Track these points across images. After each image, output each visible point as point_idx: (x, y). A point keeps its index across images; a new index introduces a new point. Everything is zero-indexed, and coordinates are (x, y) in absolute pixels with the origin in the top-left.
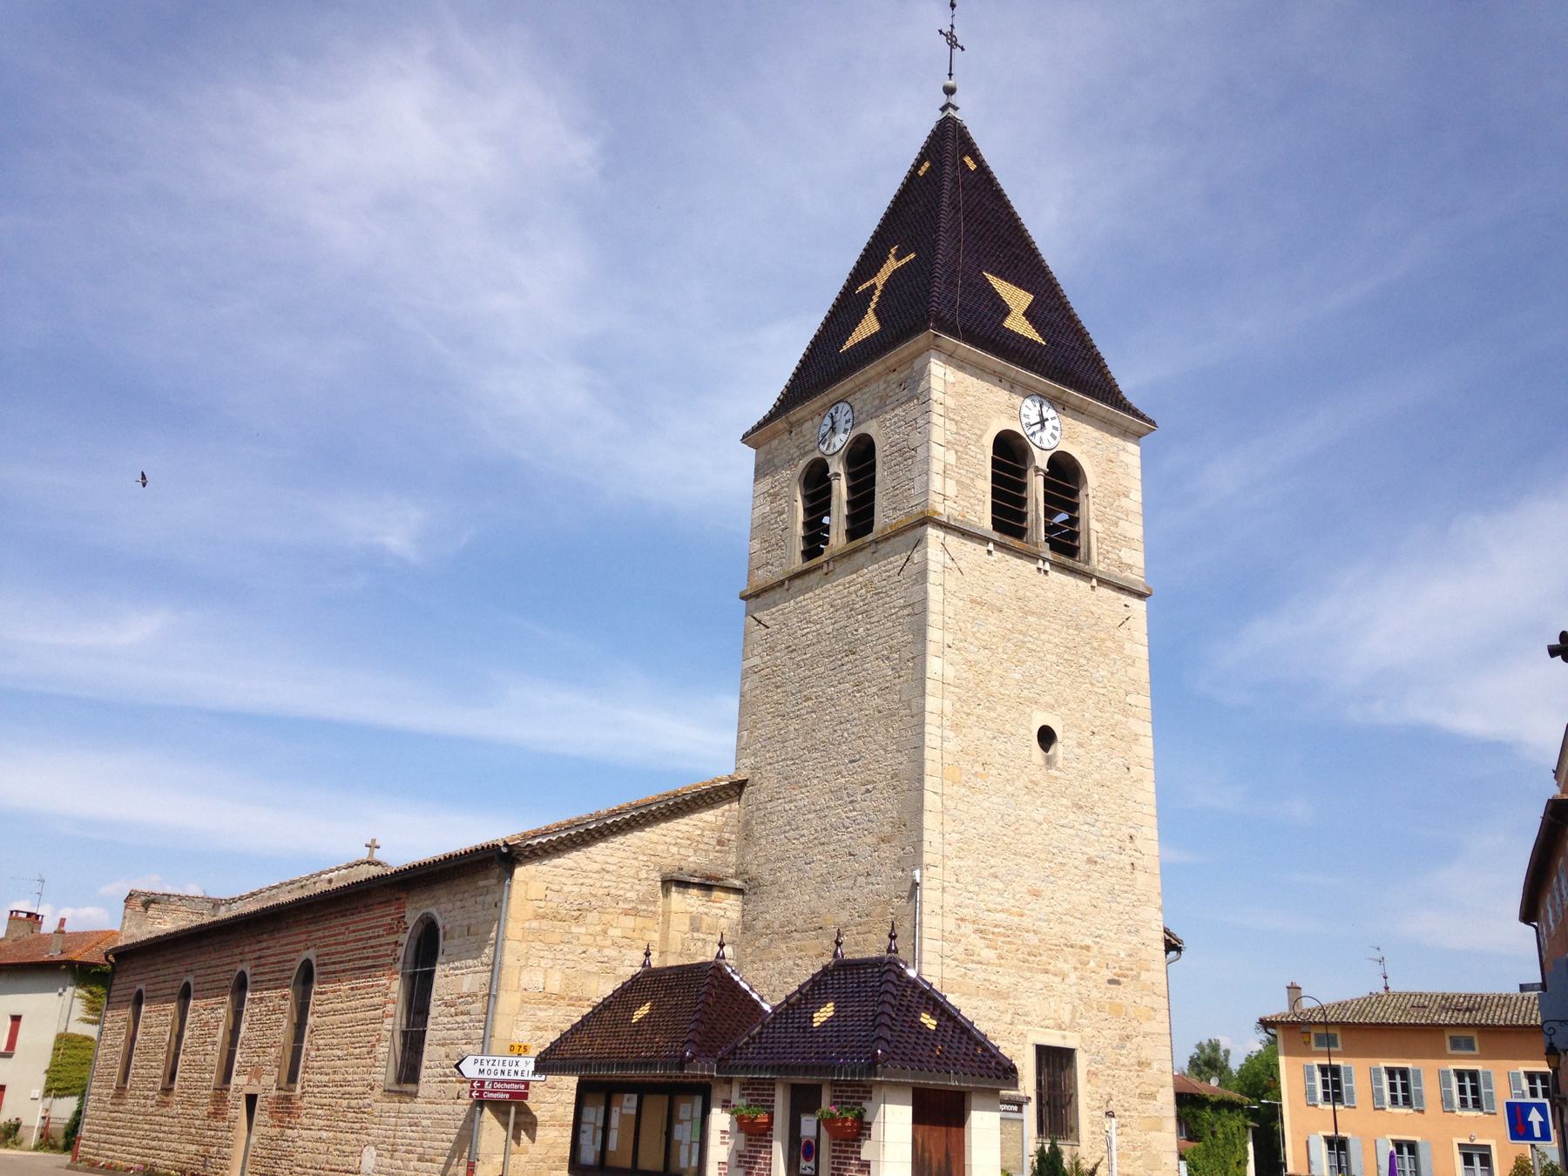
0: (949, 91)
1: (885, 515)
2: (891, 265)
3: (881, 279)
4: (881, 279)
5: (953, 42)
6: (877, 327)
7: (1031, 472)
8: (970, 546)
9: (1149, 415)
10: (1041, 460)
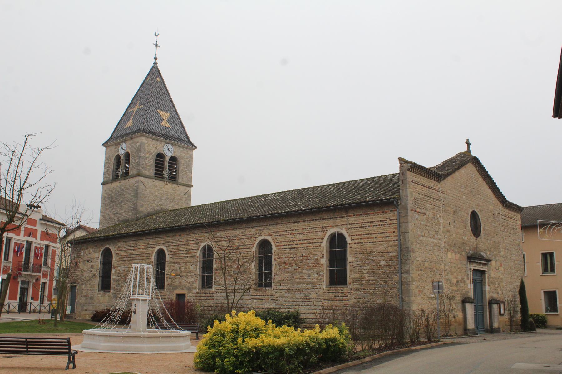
0: (156, 59)
1: (131, 172)
3: (135, 109)
4: (135, 109)
5: (156, 45)
6: (132, 124)
8: (150, 180)
10: (168, 159)
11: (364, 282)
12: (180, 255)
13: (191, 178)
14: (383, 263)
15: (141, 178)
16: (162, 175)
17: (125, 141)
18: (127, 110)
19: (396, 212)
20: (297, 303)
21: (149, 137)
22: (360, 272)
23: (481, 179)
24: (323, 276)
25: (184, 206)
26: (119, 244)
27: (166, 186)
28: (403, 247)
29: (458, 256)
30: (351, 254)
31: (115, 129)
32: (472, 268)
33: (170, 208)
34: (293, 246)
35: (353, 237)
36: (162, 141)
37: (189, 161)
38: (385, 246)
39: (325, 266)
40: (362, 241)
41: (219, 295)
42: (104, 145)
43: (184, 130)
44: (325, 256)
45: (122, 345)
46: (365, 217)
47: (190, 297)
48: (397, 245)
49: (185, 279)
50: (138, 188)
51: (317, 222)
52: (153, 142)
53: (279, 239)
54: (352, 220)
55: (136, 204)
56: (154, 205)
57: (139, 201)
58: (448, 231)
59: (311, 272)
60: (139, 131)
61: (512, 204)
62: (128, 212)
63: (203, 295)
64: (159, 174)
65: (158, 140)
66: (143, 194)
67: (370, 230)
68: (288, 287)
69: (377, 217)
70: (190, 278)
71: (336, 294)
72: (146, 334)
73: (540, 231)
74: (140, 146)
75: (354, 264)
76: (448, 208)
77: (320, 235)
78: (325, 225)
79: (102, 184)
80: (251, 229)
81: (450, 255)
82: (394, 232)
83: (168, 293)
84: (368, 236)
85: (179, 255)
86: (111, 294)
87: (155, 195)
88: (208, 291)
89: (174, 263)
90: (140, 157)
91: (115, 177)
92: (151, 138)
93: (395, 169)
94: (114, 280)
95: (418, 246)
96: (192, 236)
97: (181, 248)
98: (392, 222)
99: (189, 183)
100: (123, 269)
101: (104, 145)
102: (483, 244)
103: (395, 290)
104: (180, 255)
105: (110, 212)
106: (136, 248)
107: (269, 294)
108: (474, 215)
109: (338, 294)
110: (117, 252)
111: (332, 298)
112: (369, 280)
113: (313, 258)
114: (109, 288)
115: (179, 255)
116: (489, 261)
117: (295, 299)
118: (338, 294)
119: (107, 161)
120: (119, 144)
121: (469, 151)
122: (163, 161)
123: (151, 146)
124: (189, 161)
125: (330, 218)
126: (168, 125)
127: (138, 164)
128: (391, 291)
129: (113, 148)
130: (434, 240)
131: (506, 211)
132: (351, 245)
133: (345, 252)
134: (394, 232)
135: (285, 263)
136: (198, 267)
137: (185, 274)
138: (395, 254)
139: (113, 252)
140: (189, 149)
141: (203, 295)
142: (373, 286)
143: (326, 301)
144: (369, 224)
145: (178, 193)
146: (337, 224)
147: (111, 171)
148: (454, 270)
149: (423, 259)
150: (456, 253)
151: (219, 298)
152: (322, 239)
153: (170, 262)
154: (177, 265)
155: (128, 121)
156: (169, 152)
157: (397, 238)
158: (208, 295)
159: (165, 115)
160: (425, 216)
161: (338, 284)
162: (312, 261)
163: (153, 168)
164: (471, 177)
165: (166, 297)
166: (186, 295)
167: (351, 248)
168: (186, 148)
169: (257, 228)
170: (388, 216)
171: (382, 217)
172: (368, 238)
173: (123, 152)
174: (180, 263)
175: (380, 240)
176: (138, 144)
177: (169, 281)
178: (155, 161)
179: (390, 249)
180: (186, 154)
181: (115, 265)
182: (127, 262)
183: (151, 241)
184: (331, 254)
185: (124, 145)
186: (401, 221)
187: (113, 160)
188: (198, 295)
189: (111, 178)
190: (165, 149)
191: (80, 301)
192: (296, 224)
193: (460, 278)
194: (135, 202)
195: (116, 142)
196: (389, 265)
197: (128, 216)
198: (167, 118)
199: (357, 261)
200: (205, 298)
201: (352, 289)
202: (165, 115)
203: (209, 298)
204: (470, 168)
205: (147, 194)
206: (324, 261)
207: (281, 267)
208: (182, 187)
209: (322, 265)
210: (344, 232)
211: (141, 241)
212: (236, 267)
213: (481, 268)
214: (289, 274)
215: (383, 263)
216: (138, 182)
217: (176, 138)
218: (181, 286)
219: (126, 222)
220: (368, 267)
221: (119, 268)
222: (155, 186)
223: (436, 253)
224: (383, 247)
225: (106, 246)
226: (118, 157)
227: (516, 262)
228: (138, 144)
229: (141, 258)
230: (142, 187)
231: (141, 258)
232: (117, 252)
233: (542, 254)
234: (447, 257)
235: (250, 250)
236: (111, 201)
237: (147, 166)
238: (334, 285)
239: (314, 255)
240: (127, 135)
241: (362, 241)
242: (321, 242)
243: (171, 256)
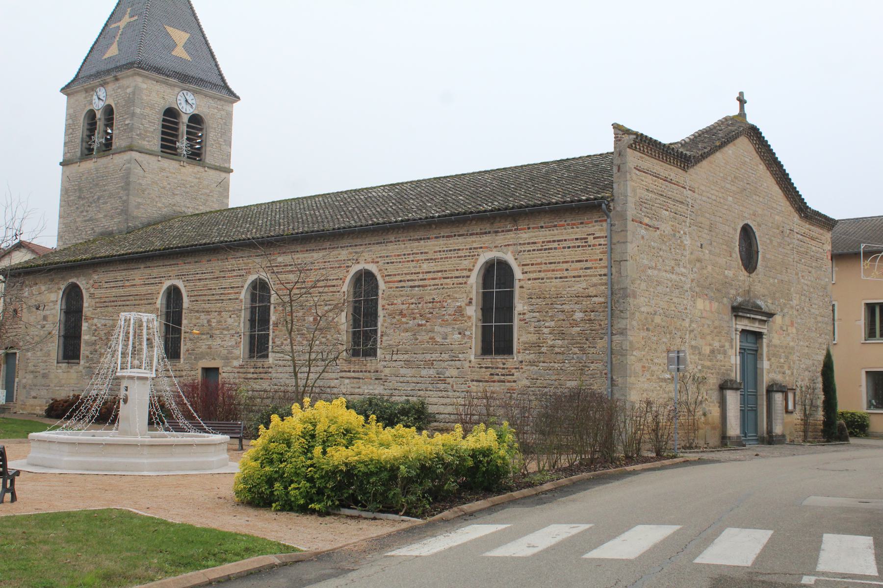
1: (116, 143)
2: (126, 19)
3: (122, 24)
4: (122, 24)
7: (181, 124)
8: (153, 159)
9: (238, 94)
10: (185, 119)
11: (544, 349)
12: (210, 298)
13: (229, 155)
14: (578, 316)
15: (135, 155)
16: (175, 149)
17: (103, 84)
18: (106, 25)
19: (604, 224)
20: (423, 386)
22: (538, 331)
23: (762, 167)
24: (470, 338)
25: (216, 207)
26: (96, 277)
27: (183, 170)
28: (616, 287)
29: (715, 305)
30: (521, 298)
31: (85, 61)
32: (740, 328)
33: (190, 211)
34: (417, 283)
35: (526, 269)
36: (175, 86)
37: (225, 124)
38: (584, 285)
39: (474, 319)
40: (542, 275)
41: (280, 370)
43: (217, 65)
44: (474, 302)
45: (103, 459)
46: (548, 233)
47: (226, 375)
48: (606, 284)
49: (219, 341)
50: (129, 173)
51: (461, 239)
52: (158, 87)
53: (391, 269)
54: (525, 236)
55: (125, 202)
56: (159, 205)
57: (131, 197)
58: (699, 260)
59: (448, 329)
60: (130, 65)
61: (817, 213)
62: (112, 217)
63: (252, 370)
64: (168, 147)
65: (166, 84)
66: (140, 184)
67: (557, 255)
68: (406, 356)
69: (569, 232)
70: (227, 339)
71: (493, 371)
72: (147, 440)
73: (864, 264)
74: (134, 93)
75: (526, 316)
76: (700, 219)
77: (466, 263)
78: (475, 245)
79: (61, 164)
80: (340, 251)
81: (700, 304)
82: (601, 260)
83: (187, 367)
84: (553, 266)
85: (207, 298)
86: (81, 368)
87: (162, 187)
88: (260, 362)
89: (197, 312)
90: (133, 115)
91: (87, 152)
92: (154, 80)
93: (606, 144)
94: (87, 343)
95: (643, 286)
97: (212, 284)
98: (597, 242)
99: (226, 165)
100: (103, 322)
101: (63, 90)
102: (761, 286)
103: (600, 366)
104: (210, 298)
105: (78, 217)
106: (127, 284)
107: (373, 369)
108: (747, 232)
109: (497, 371)
110: (92, 290)
111: (487, 378)
112: (553, 346)
113: (452, 306)
114: (78, 358)
115: (207, 298)
116: (771, 315)
117: (419, 379)
118: (497, 371)
119: (70, 122)
120: (93, 89)
121: (742, 114)
122: (177, 123)
123: (154, 94)
124: (225, 124)
125: (486, 233)
126: (185, 56)
127: (130, 129)
128: (592, 366)
129: (81, 97)
130: (674, 277)
131: (805, 227)
132: (522, 283)
133: (510, 295)
134: (601, 260)
135: (401, 313)
136: (242, 320)
137: (218, 332)
138: (602, 300)
139: (84, 291)
140: (226, 101)
141: (252, 370)
142: (560, 357)
143: (474, 383)
144: (555, 245)
145: (206, 183)
146: (498, 243)
147: (79, 141)
148: (707, 331)
149: (651, 310)
150: (711, 299)
151: (281, 375)
152: (470, 270)
153: (191, 311)
154: (203, 316)
155: (108, 46)
156: (189, 107)
158: (261, 370)
159: (180, 37)
160: (658, 232)
161: (499, 352)
162: (451, 311)
163: (158, 136)
164: (744, 163)
165: (184, 373)
166: (221, 371)
167: (522, 287)
168: (220, 99)
169: (350, 250)
170: (591, 230)
171: (579, 232)
172: (553, 270)
173: (101, 104)
175: (576, 273)
176: (129, 91)
177: (189, 345)
178: (161, 123)
179: (592, 291)
180: (219, 110)
181: (89, 314)
182: (110, 309)
183: (155, 272)
184: (486, 298)
185: (101, 92)
186: (614, 241)
187: (81, 121)
188: (241, 370)
189: (79, 154)
190: (181, 99)
191: (24, 381)
192: (422, 242)
193: (716, 344)
194: (125, 198)
195: (86, 85)
196: (590, 320)
197: (112, 224)
198: (184, 41)
199: (532, 311)
200: (255, 376)
201: (521, 362)
202: (180, 37)
203: (262, 375)
204: (743, 146)
205: (148, 185)
206: (473, 312)
207: (395, 320)
208: (212, 173)
209: (470, 318)
210: (509, 258)
211: (136, 271)
212: (311, 319)
213: (755, 327)
214: (410, 334)
215: (578, 316)
217: (202, 80)
218: (210, 353)
219: (107, 235)
220: (553, 324)
221: (95, 321)
222: (162, 170)
223: (675, 300)
224: (579, 287)
225: (70, 281)
226: (91, 115)
227: (819, 319)
228: (129, 91)
229: (137, 302)
231: (137, 302)
232: (92, 290)
233: (867, 304)
234: (694, 307)
235: (338, 289)
236: (80, 197)
237: (146, 131)
238: (491, 353)
239: (455, 299)
240: (108, 72)
241: (542, 275)
242: (468, 277)
243: (193, 299)
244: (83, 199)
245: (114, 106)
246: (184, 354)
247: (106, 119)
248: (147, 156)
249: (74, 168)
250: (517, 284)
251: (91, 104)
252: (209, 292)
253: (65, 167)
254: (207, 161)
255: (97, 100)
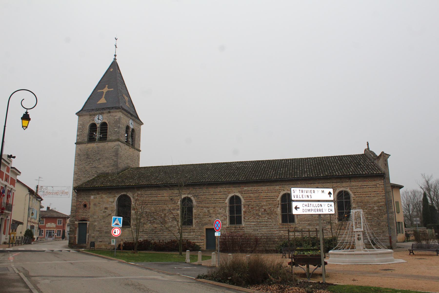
0: (115, 56)
1: (109, 137)
8: (124, 145)
15: (120, 143)
16: (94, 139)
18: (95, 90)
19: (382, 181)
21: (109, 112)
26: (139, 193)
35: (356, 194)
36: (128, 117)
40: (361, 196)
41: (248, 228)
42: (77, 114)
43: (135, 111)
45: (384, 258)
52: (125, 117)
63: (234, 229)
65: (127, 116)
67: (366, 190)
68: (309, 222)
69: (371, 183)
72: (363, 252)
79: (75, 143)
84: (365, 193)
88: (238, 226)
89: (202, 207)
90: (119, 127)
96: (219, 189)
98: (380, 186)
101: (77, 114)
103: (385, 223)
105: (87, 166)
106: (159, 195)
107: (294, 227)
112: (368, 218)
120: (95, 115)
121: (368, 148)
128: (382, 223)
138: (383, 203)
139: (132, 198)
141: (234, 229)
142: (370, 221)
144: (366, 187)
146: (343, 185)
154: (205, 209)
157: (384, 195)
159: (126, 98)
165: (196, 231)
169: (280, 186)
170: (377, 183)
171: (374, 183)
173: (100, 122)
174: (208, 207)
176: (116, 118)
179: (380, 201)
187: (88, 127)
191: (93, 235)
194: (115, 160)
195: (91, 113)
197: (109, 170)
203: (239, 231)
208: (136, 151)
210: (348, 190)
211: (164, 191)
212: (263, 210)
215: (376, 208)
216: (118, 145)
219: (105, 175)
220: (367, 211)
224: (375, 199)
225: (122, 194)
230: (120, 149)
235: (276, 199)
240: (103, 109)
241: (361, 196)
244: (89, 159)
245: (107, 123)
246: (195, 223)
247: (101, 128)
248: (122, 144)
249: (83, 146)
250: (352, 199)
251: (94, 120)
252: (208, 200)
253: (78, 145)
254: (136, 147)
255: (97, 119)
